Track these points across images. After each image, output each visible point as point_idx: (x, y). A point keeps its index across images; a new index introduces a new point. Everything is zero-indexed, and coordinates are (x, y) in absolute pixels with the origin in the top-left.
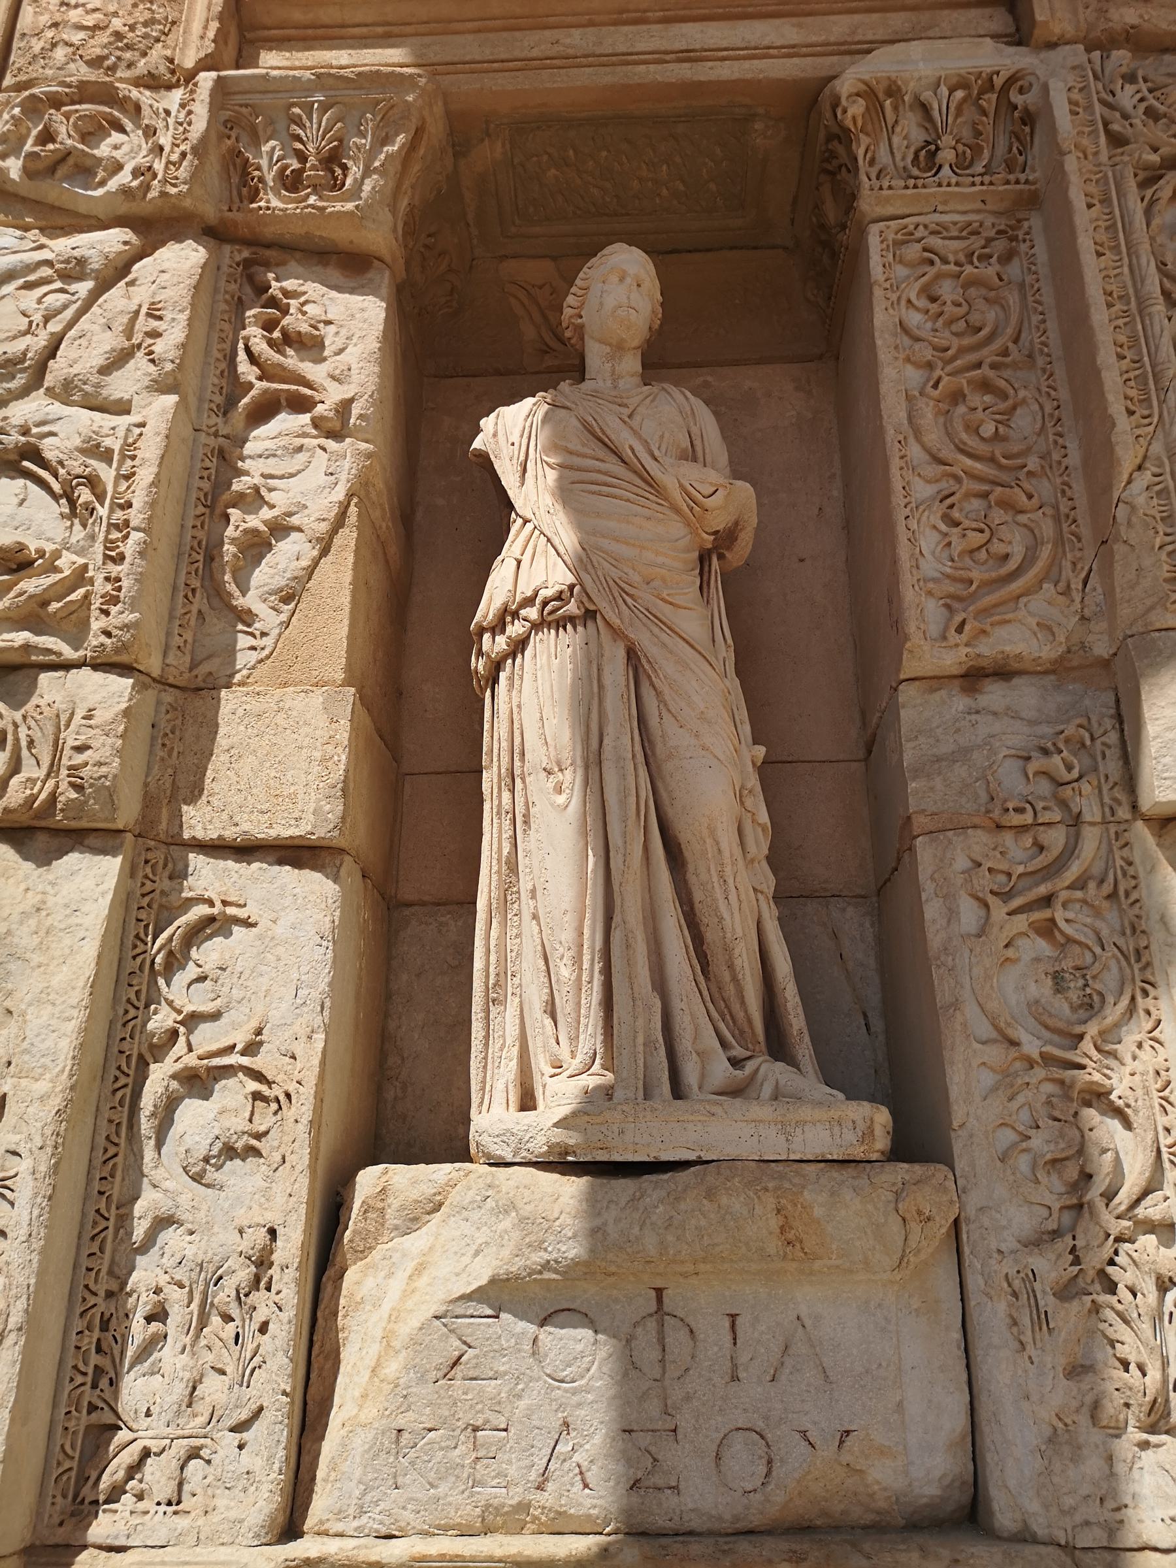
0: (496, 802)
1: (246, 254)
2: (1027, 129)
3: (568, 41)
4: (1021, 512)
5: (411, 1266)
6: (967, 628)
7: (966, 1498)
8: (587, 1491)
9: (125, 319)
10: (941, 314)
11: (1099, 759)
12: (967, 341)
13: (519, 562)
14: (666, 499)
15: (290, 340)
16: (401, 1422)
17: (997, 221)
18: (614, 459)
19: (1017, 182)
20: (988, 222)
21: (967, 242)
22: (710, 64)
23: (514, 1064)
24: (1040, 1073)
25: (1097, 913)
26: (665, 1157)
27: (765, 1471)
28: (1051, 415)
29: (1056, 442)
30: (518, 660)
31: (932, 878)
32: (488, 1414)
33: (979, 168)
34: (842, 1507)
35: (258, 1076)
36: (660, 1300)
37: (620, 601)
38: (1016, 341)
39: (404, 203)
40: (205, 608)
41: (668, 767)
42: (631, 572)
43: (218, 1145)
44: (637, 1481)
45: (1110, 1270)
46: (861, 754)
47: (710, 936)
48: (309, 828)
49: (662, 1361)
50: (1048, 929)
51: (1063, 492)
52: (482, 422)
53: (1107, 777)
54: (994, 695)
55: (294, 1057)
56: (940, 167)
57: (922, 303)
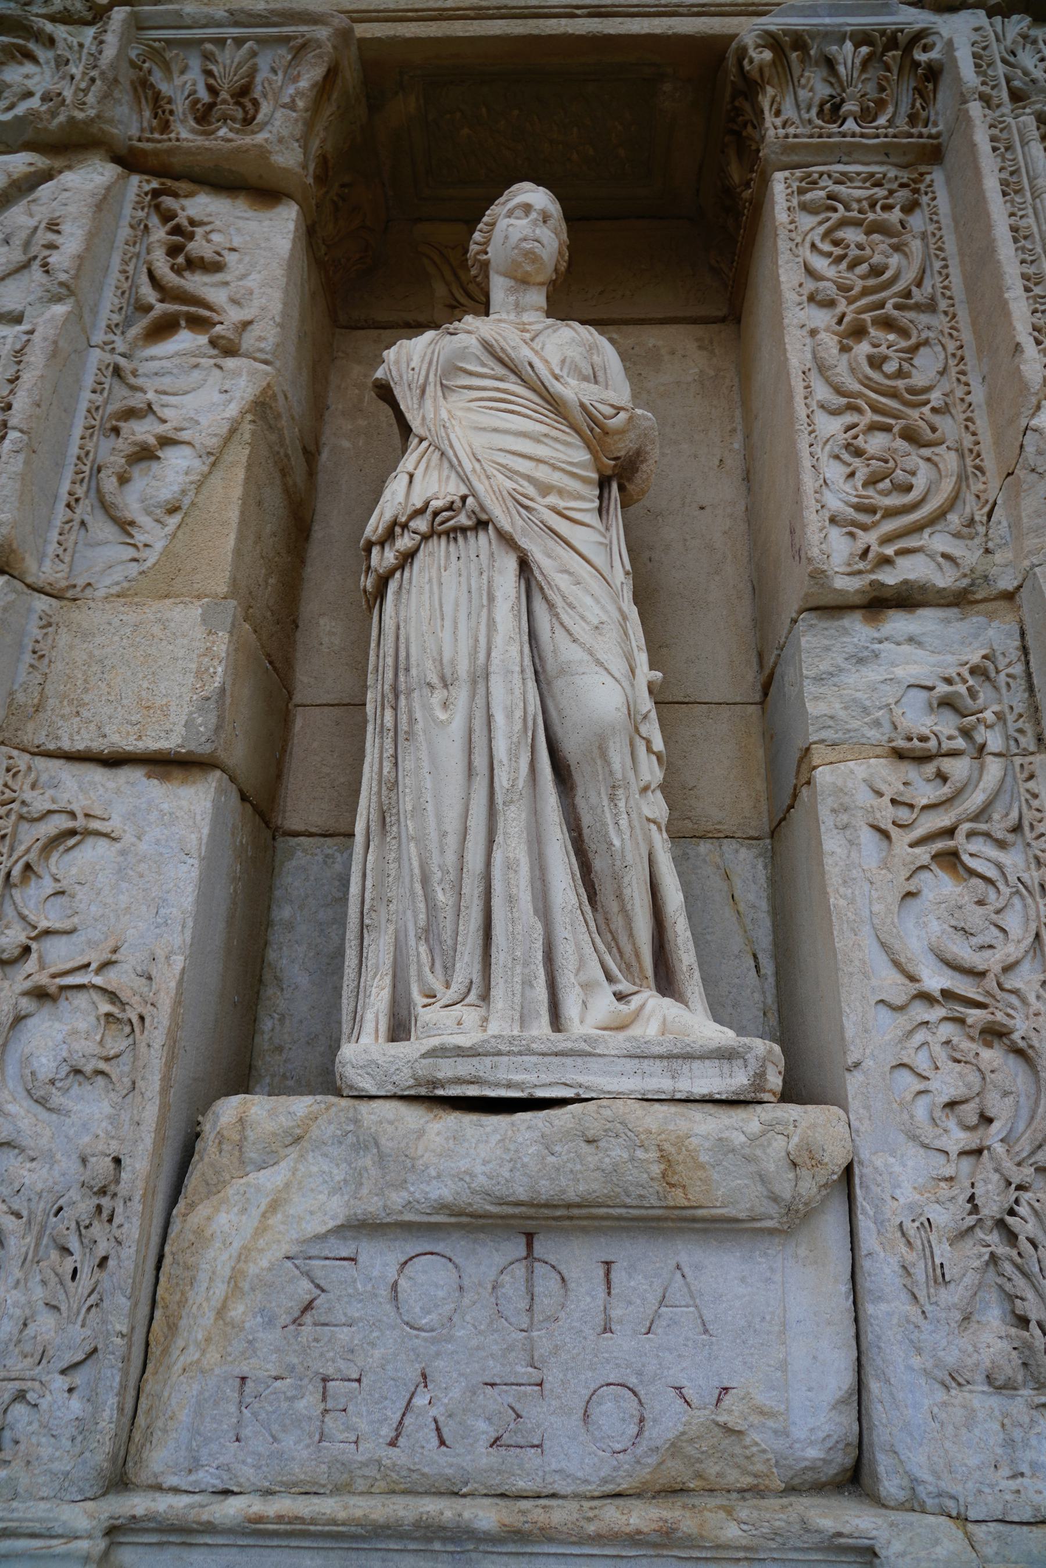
0: (379, 722)
1: (155, 184)
2: (930, 86)
4: (924, 446)
5: (264, 1203)
6: (871, 555)
8: (443, 1448)
10: (844, 256)
11: (1004, 690)
12: (871, 282)
13: (411, 476)
14: (565, 419)
15: (195, 264)
16: (245, 1369)
17: (900, 174)
18: (513, 378)
19: (921, 136)
21: (871, 192)
22: (620, 20)
23: (386, 994)
25: (1002, 845)
26: (540, 1093)
27: (636, 1430)
28: (954, 355)
29: (958, 380)
30: (406, 574)
31: (833, 811)
32: (341, 1364)
33: (882, 121)
34: (717, 1468)
35: (112, 996)
36: (530, 1246)
37: (514, 512)
38: (919, 285)
39: (315, 144)
40: (88, 518)
41: (559, 684)
42: (525, 484)
43: (65, 1069)
44: (497, 1439)
45: (1010, 1220)
46: (757, 698)
47: (598, 864)
48: (180, 741)
49: (530, 1310)
50: (950, 860)
51: (967, 427)
53: (1011, 708)
54: (898, 623)
55: (150, 978)
57: (826, 247)
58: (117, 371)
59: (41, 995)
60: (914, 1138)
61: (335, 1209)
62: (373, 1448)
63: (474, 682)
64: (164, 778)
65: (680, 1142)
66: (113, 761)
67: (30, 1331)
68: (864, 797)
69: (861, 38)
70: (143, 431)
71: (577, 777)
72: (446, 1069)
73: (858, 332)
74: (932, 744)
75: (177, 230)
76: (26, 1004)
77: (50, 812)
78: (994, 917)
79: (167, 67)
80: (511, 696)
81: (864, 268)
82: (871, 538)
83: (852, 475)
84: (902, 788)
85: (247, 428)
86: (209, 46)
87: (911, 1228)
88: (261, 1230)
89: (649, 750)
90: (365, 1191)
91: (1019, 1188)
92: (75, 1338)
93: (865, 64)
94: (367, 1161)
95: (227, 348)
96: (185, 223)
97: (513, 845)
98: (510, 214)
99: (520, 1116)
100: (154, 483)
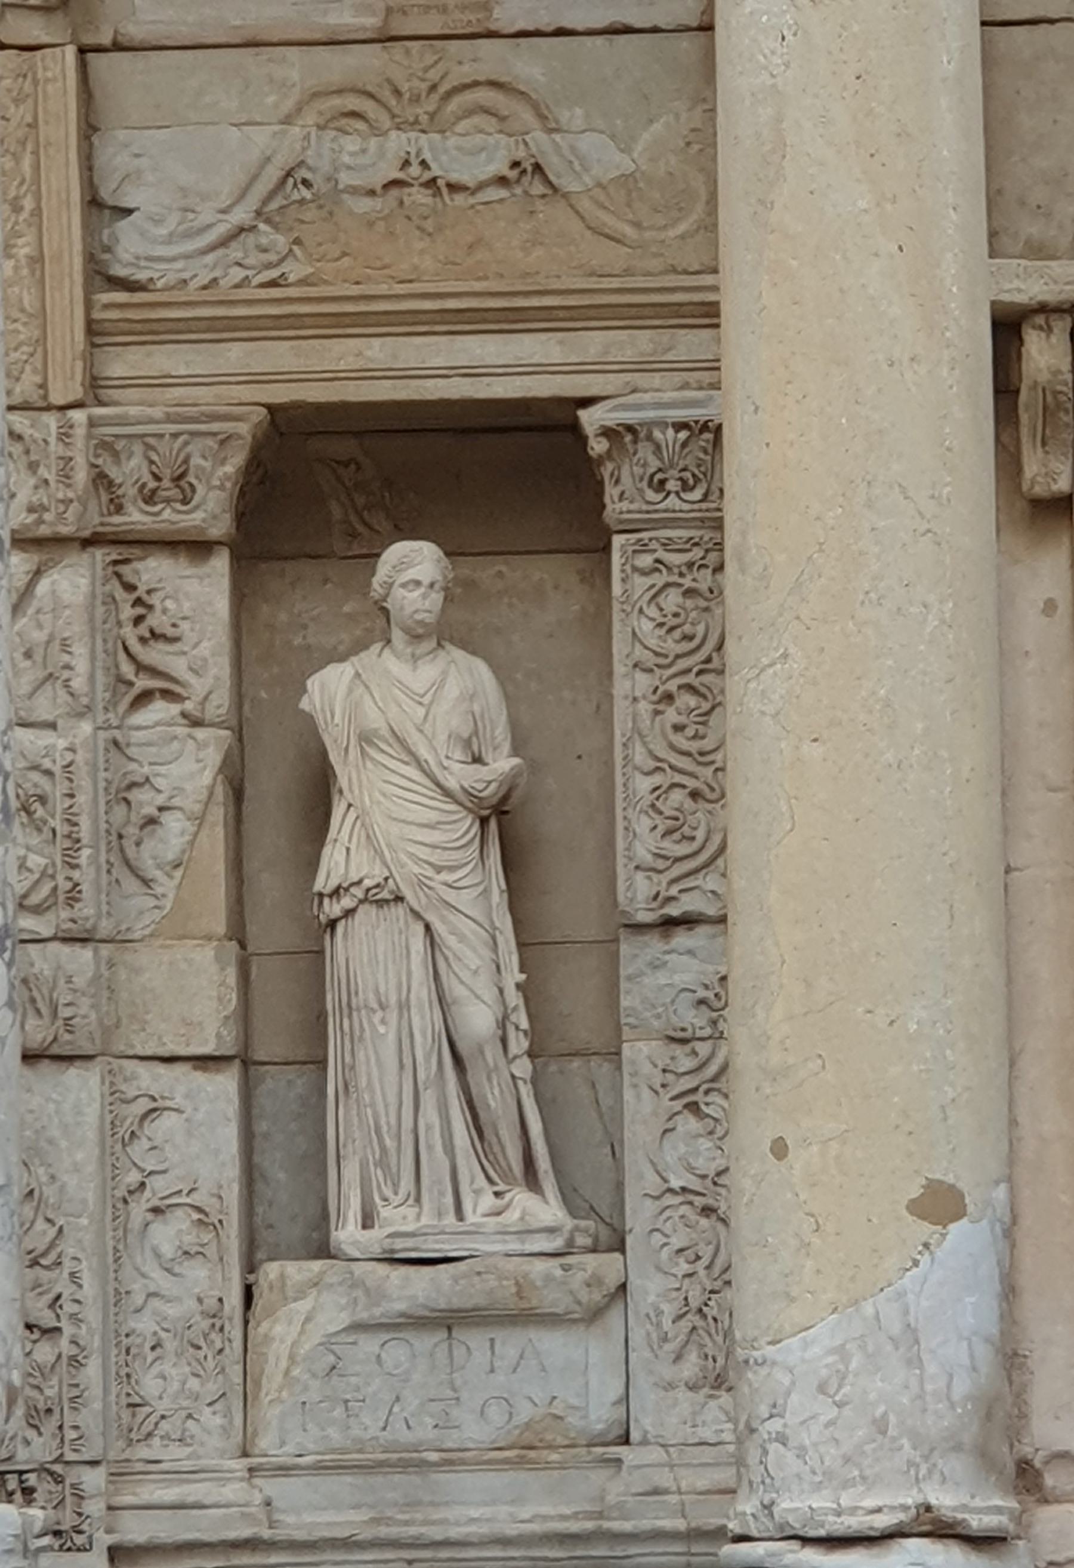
1: (114, 557)
3: (369, 353)
7: (622, 1432)
9: (41, 651)
13: (348, 849)
20: (706, 538)
21: (691, 554)
23: (359, 1200)
24: (679, 1199)
33: (697, 494)
35: (199, 1209)
41: (453, 1008)
43: (180, 1253)
45: (705, 1309)
47: (482, 1115)
50: (693, 1108)
52: (309, 683)
54: (682, 939)
55: (220, 1197)
56: (668, 494)
57: (652, 611)
58: (116, 743)
59: (156, 1210)
60: (658, 1268)
61: (344, 1319)
62: (373, 1432)
63: (400, 1008)
64: (205, 1070)
65: (526, 1276)
66: (170, 1059)
67: (187, 1386)
68: (646, 1068)
69: (679, 426)
70: (145, 801)
71: (468, 1067)
72: (399, 1244)
73: (669, 698)
74: (688, 1034)
75: (138, 602)
76: (150, 1216)
77: (137, 1097)
78: (718, 1143)
79: (116, 455)
80: (425, 1021)
81: (677, 634)
82: (665, 878)
83: (655, 827)
84: (669, 1061)
85: (219, 790)
86: (151, 441)
87: (652, 1315)
88: (302, 1332)
89: (517, 1028)
90: (359, 1308)
91: (712, 1292)
92: (213, 1388)
93: (684, 445)
94: (359, 1293)
95: (197, 723)
96: (145, 597)
97: (430, 1114)
98: (404, 585)
99: (441, 1267)
100: (160, 846)
